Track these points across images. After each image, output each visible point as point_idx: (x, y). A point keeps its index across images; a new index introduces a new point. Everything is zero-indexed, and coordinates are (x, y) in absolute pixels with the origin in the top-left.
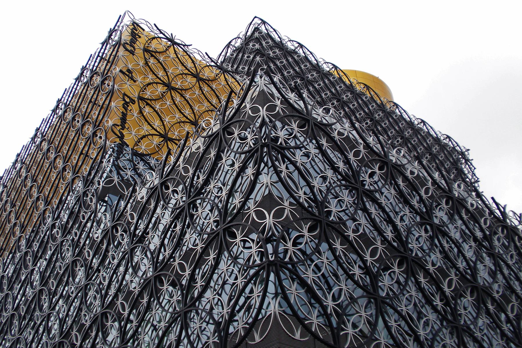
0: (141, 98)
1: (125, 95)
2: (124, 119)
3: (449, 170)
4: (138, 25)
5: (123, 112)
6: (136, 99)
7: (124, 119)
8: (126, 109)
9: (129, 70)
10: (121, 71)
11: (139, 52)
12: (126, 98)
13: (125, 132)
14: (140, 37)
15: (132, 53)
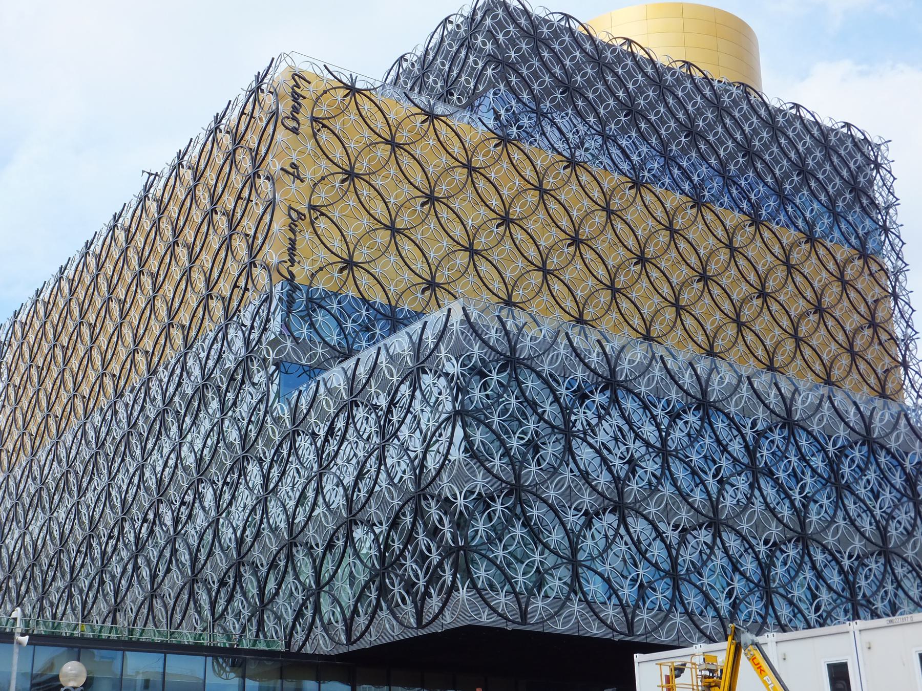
0: (312, 207)
1: (290, 208)
2: (292, 249)
3: (813, 222)
4: (299, 77)
5: (290, 239)
6: (306, 212)
7: (292, 249)
8: (293, 232)
9: (293, 164)
10: (282, 169)
11: (305, 128)
12: (292, 213)
13: (295, 270)
14: (304, 98)
15: (295, 131)
